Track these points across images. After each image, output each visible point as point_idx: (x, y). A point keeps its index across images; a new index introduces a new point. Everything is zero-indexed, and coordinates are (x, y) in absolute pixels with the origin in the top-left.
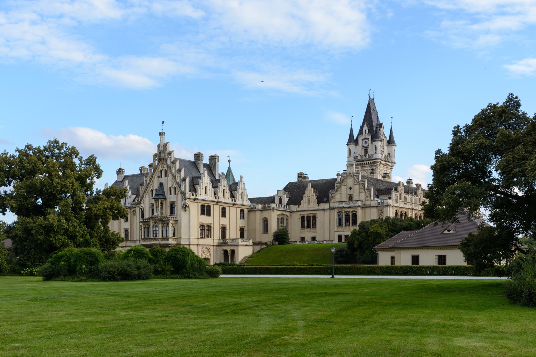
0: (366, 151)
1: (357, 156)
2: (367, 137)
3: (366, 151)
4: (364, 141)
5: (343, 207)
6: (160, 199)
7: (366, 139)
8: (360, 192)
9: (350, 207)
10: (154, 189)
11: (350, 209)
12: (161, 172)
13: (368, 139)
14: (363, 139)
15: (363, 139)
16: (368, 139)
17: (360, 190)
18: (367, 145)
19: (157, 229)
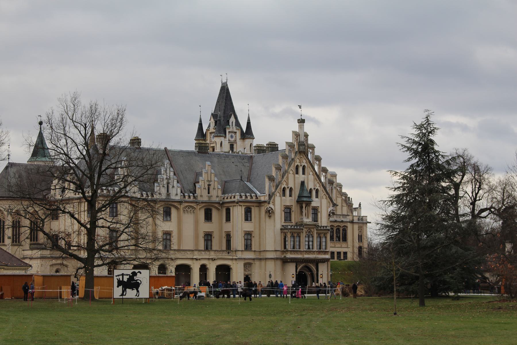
0: (232, 147)
1: (228, 151)
2: (235, 131)
3: (232, 147)
4: (230, 134)
5: (336, 221)
6: (304, 202)
7: (232, 132)
8: (342, 206)
9: (342, 221)
10: (288, 187)
11: (342, 224)
12: (297, 168)
13: (235, 133)
14: (229, 132)
15: (229, 132)
16: (235, 133)
17: (342, 204)
18: (233, 139)
19: (311, 239)
